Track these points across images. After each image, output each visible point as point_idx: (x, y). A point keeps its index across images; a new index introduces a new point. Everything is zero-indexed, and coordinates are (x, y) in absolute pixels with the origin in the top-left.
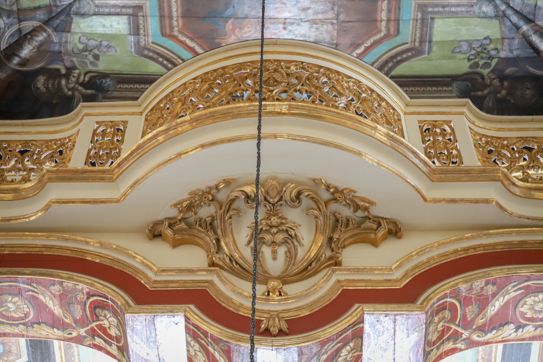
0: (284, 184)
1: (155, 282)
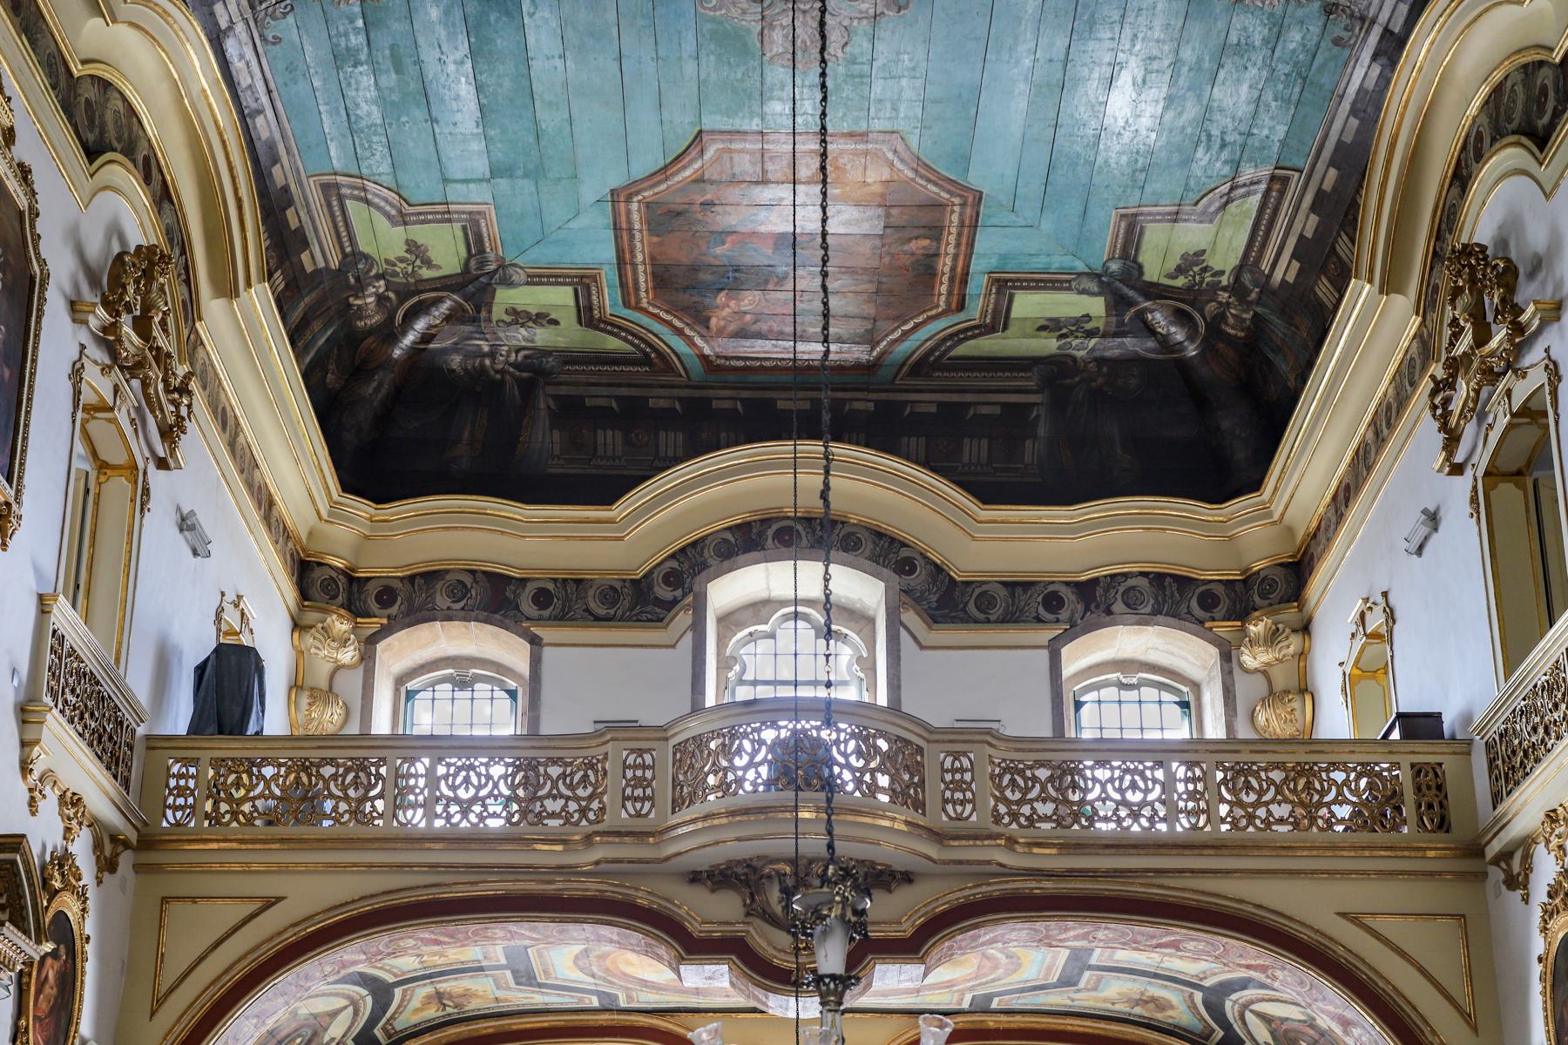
0: (811, 861)
1: (701, 932)
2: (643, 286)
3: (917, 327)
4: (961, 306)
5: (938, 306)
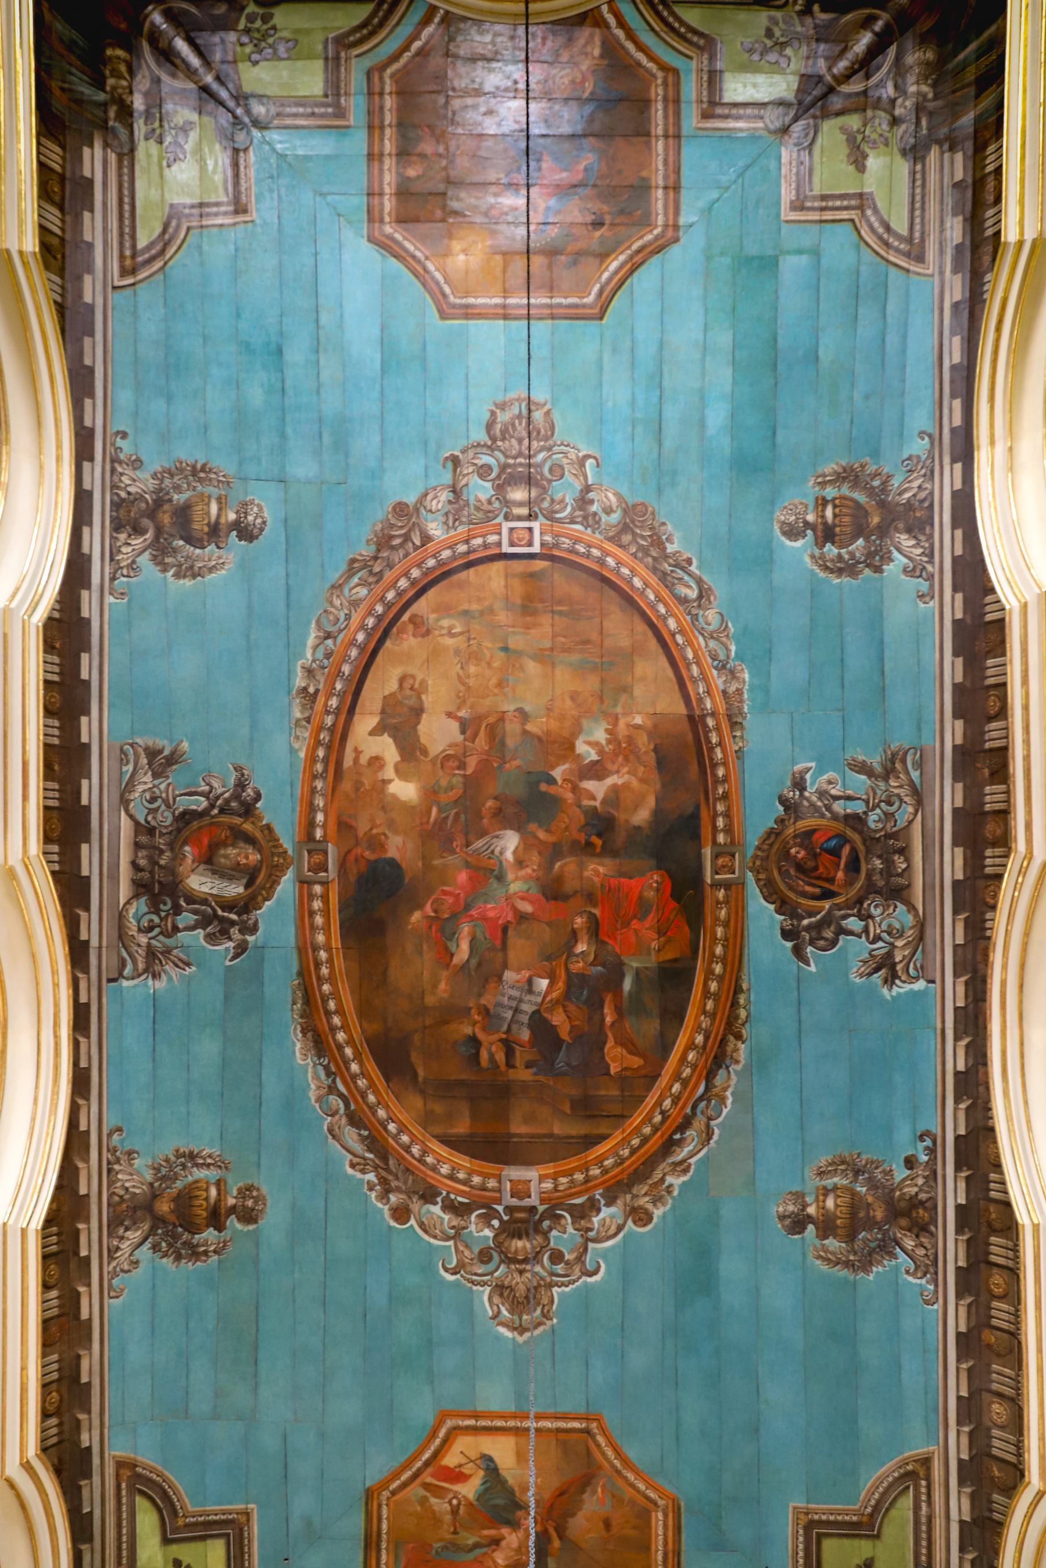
2: (660, 106)
3: (406, 48)
4: (369, 74)
5: (392, 76)
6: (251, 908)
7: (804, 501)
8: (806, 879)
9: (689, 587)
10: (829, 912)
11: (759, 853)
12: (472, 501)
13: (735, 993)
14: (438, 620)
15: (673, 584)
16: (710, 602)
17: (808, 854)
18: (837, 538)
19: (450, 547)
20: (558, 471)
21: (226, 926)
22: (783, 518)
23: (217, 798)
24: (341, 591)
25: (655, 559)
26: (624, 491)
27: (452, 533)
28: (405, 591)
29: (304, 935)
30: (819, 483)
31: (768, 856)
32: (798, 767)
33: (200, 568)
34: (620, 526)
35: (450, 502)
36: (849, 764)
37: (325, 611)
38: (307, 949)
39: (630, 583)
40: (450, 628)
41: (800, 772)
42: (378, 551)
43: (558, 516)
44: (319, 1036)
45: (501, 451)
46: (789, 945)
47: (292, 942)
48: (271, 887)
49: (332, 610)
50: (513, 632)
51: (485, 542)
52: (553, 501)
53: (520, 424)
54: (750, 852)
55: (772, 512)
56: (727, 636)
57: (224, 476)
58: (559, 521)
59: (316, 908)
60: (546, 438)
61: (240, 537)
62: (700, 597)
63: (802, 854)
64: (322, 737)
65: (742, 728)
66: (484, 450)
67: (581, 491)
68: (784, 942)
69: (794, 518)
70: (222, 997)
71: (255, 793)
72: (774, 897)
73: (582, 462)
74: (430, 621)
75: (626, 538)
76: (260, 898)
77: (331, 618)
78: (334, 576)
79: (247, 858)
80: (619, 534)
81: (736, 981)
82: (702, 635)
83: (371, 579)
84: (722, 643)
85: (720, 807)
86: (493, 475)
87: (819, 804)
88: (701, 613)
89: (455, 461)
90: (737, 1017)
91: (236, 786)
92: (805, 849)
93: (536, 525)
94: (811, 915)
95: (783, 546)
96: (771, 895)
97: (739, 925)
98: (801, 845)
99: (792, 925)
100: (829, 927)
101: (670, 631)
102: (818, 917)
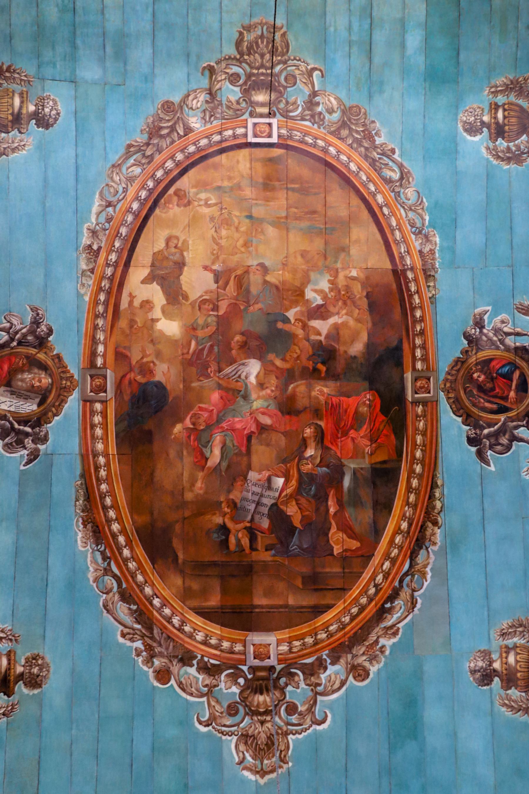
6: (42, 423)
7: (481, 106)
8: (486, 397)
9: (393, 171)
10: (504, 423)
11: (449, 377)
12: (224, 102)
13: (432, 488)
14: (197, 194)
15: (381, 168)
16: (409, 183)
17: (487, 378)
18: (506, 135)
19: (206, 137)
20: (292, 79)
21: (21, 437)
22: (465, 119)
23: (16, 333)
24: (120, 169)
25: (367, 149)
26: (343, 95)
27: (209, 126)
28: (171, 170)
29: (87, 444)
30: (493, 92)
31: (456, 379)
32: (478, 311)
33: (5, 148)
34: (340, 123)
35: (207, 102)
36: (517, 308)
37: (107, 185)
38: (88, 456)
39: (347, 167)
40: (207, 200)
41: (480, 314)
42: (150, 138)
43: (291, 114)
44: (97, 527)
45: (247, 63)
46: (474, 449)
47: (77, 450)
48: (59, 405)
49: (113, 184)
50: (256, 204)
51: (234, 133)
52: (287, 103)
53: (262, 42)
54: (442, 376)
55: (456, 114)
56: (423, 208)
57: (25, 76)
58: (292, 118)
59: (97, 422)
60: (283, 55)
61: (38, 125)
62: (402, 178)
63: (482, 377)
64: (103, 285)
65: (435, 280)
66: (234, 62)
67: (310, 95)
68: (470, 447)
69: (473, 118)
70: (16, 496)
71: (47, 329)
72: (461, 411)
73: (310, 73)
74: (191, 194)
75: (344, 133)
76: (50, 414)
77: (112, 190)
78: (114, 157)
79: (40, 381)
80: (339, 129)
81: (433, 478)
82: (404, 208)
83: (143, 161)
84: (419, 214)
85: (418, 341)
86: (241, 82)
87: (495, 338)
88: (402, 190)
89: (211, 70)
90: (434, 507)
91: (32, 323)
92: (485, 374)
93: (274, 121)
94: (489, 426)
95: (465, 140)
96: (458, 410)
97: (434, 433)
98: (481, 371)
99: (476, 434)
100: (504, 435)
101: (378, 204)
102: (496, 427)
